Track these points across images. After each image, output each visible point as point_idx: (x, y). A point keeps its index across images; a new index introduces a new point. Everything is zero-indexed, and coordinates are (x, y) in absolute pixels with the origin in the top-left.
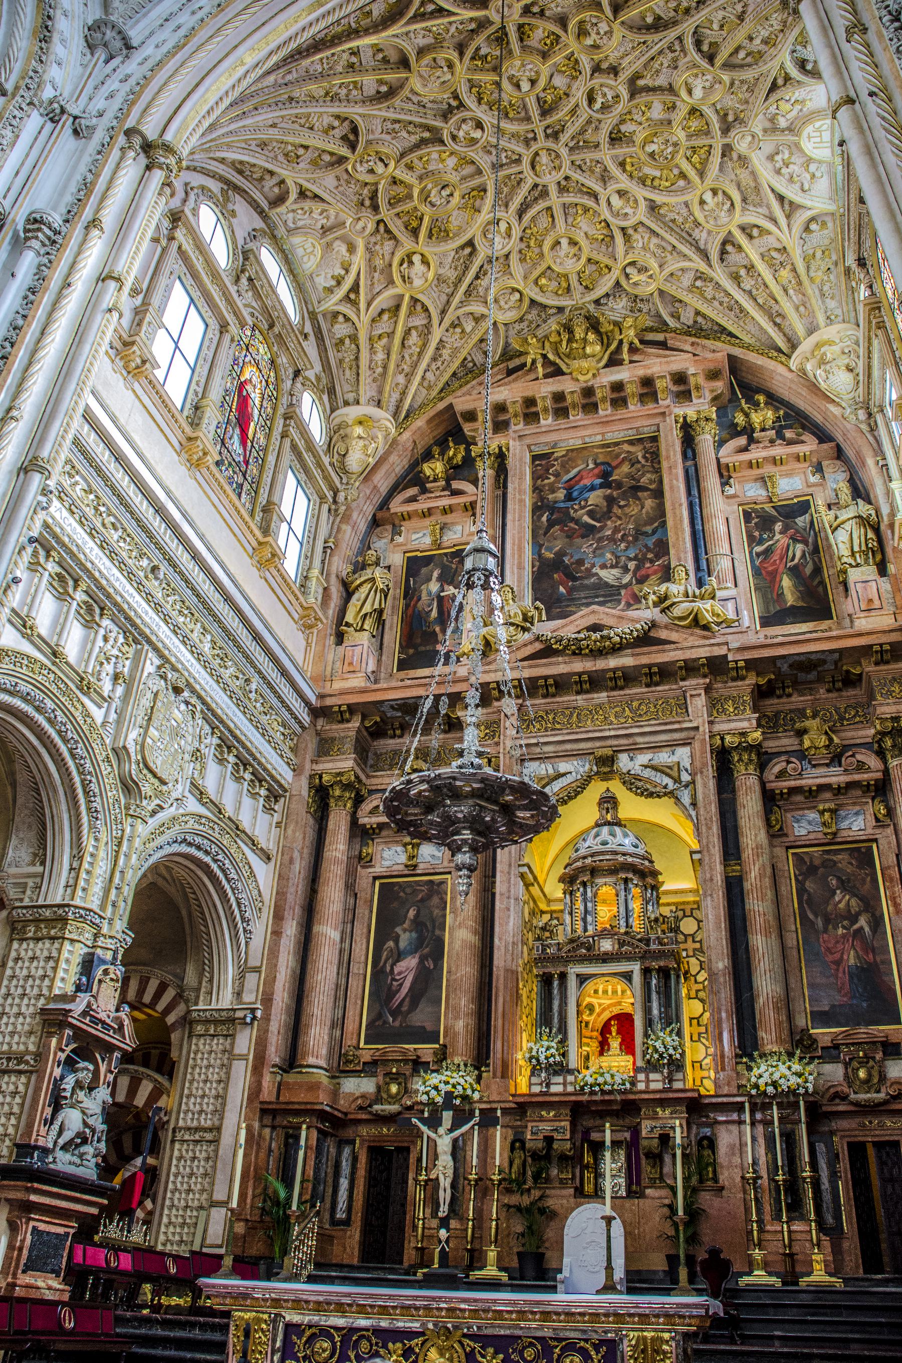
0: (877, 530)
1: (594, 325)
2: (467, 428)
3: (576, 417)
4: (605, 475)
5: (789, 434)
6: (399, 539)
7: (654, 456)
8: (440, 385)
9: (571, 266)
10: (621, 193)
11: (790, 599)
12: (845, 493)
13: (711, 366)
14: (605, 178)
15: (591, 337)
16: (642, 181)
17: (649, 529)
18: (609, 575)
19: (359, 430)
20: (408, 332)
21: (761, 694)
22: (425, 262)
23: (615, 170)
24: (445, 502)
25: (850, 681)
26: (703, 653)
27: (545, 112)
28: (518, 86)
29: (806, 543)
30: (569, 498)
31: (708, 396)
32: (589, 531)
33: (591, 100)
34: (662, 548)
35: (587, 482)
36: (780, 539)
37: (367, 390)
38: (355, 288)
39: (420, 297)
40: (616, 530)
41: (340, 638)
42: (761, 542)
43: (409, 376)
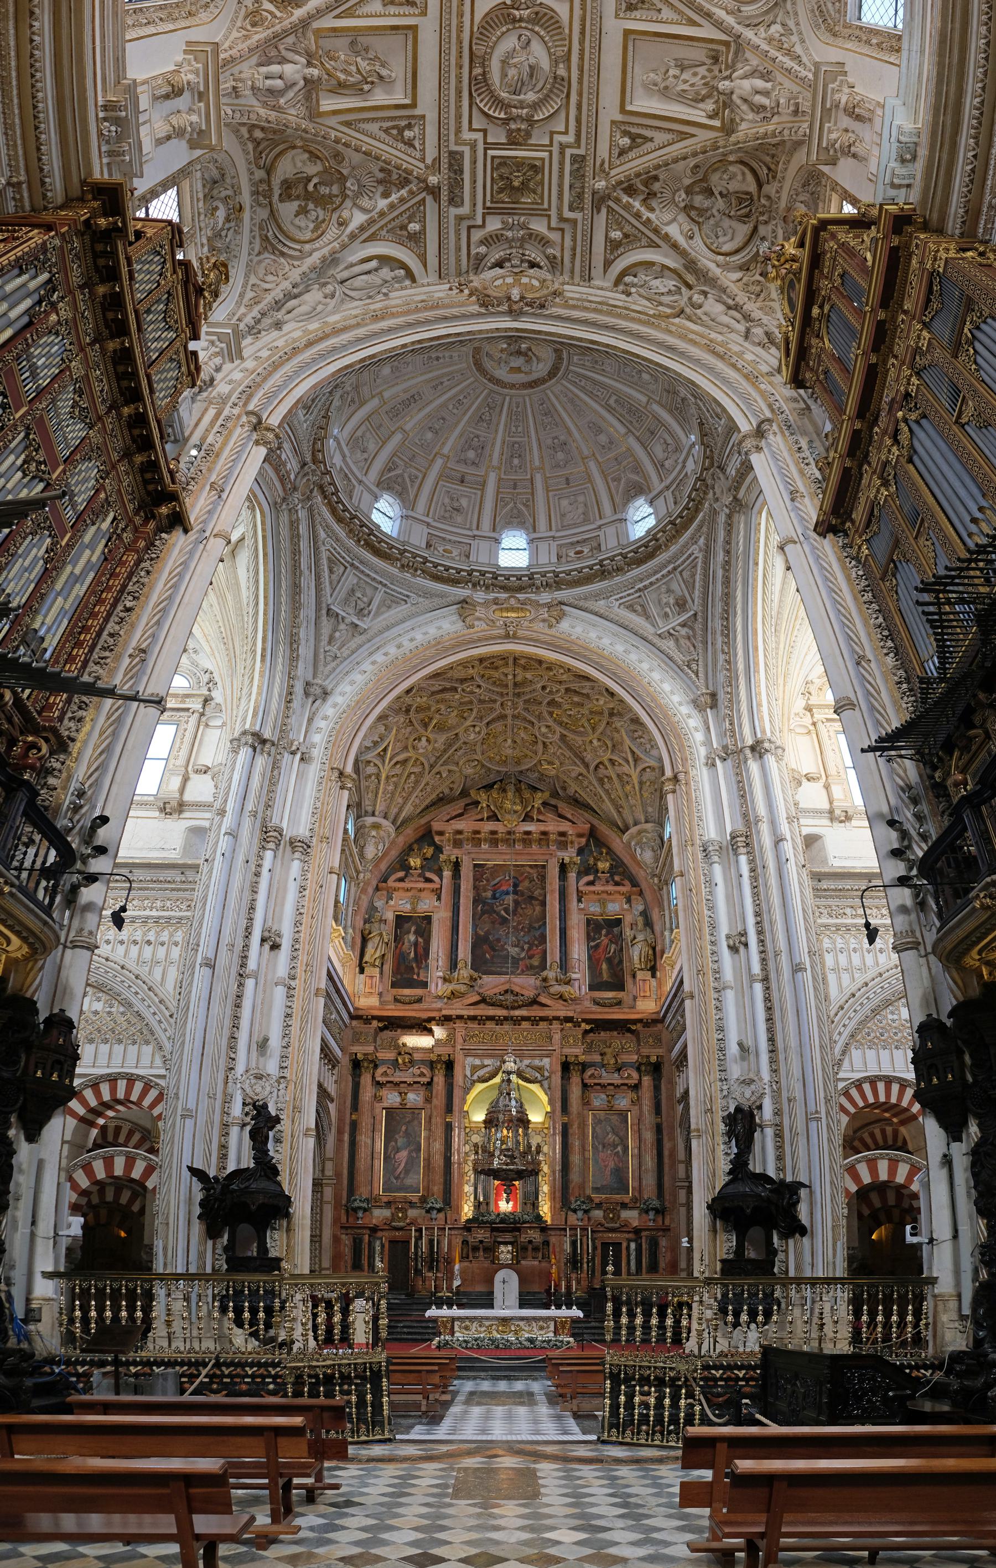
0: (654, 949)
1: (518, 790)
2: (437, 839)
3: (502, 847)
4: (515, 886)
5: (617, 878)
6: (392, 903)
7: (543, 878)
8: (423, 806)
9: (509, 752)
10: (548, 727)
11: (605, 976)
12: (640, 920)
13: (581, 831)
14: (539, 717)
15: (518, 801)
16: (560, 724)
17: (536, 925)
18: (513, 951)
19: (374, 833)
20: (409, 776)
21: (586, 1032)
22: (428, 741)
23: (545, 714)
24: (421, 885)
25: (629, 1030)
26: (562, 1014)
27: (516, 684)
28: (506, 675)
29: (616, 944)
30: (494, 897)
31: (577, 846)
32: (504, 921)
33: (544, 688)
34: (543, 940)
35: (504, 888)
36: (604, 940)
37: (380, 807)
38: (385, 750)
39: (422, 759)
40: (519, 923)
41: (362, 971)
42: (594, 940)
43: (406, 800)
